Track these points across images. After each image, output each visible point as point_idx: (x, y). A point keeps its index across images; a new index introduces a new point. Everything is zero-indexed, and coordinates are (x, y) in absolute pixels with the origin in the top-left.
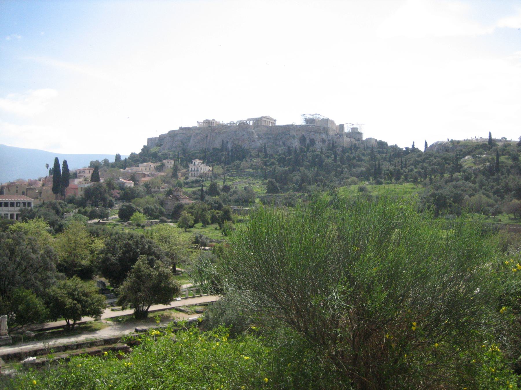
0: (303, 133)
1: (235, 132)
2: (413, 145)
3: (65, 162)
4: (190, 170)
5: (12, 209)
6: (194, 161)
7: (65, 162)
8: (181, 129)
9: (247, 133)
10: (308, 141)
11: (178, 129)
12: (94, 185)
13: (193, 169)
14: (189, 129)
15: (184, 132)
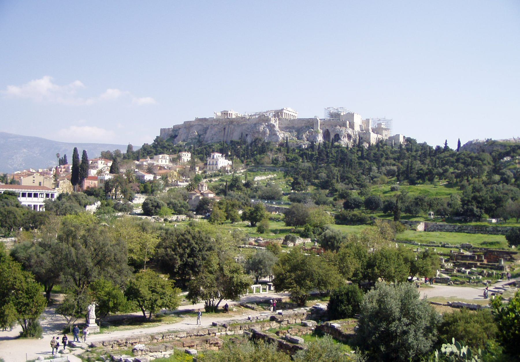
0: (327, 128)
1: (255, 124)
2: (446, 144)
3: (84, 153)
4: (208, 163)
5: (35, 199)
6: (212, 154)
7: (84, 153)
8: (198, 120)
9: (268, 126)
10: (332, 136)
11: (194, 119)
12: (115, 177)
13: (211, 163)
14: (205, 120)
15: (201, 123)
